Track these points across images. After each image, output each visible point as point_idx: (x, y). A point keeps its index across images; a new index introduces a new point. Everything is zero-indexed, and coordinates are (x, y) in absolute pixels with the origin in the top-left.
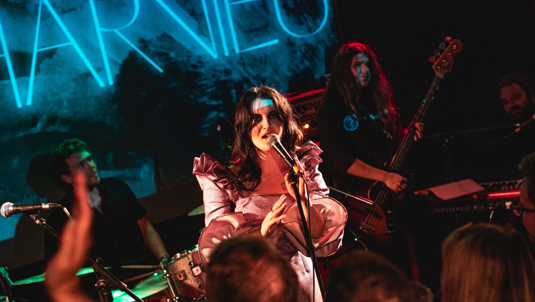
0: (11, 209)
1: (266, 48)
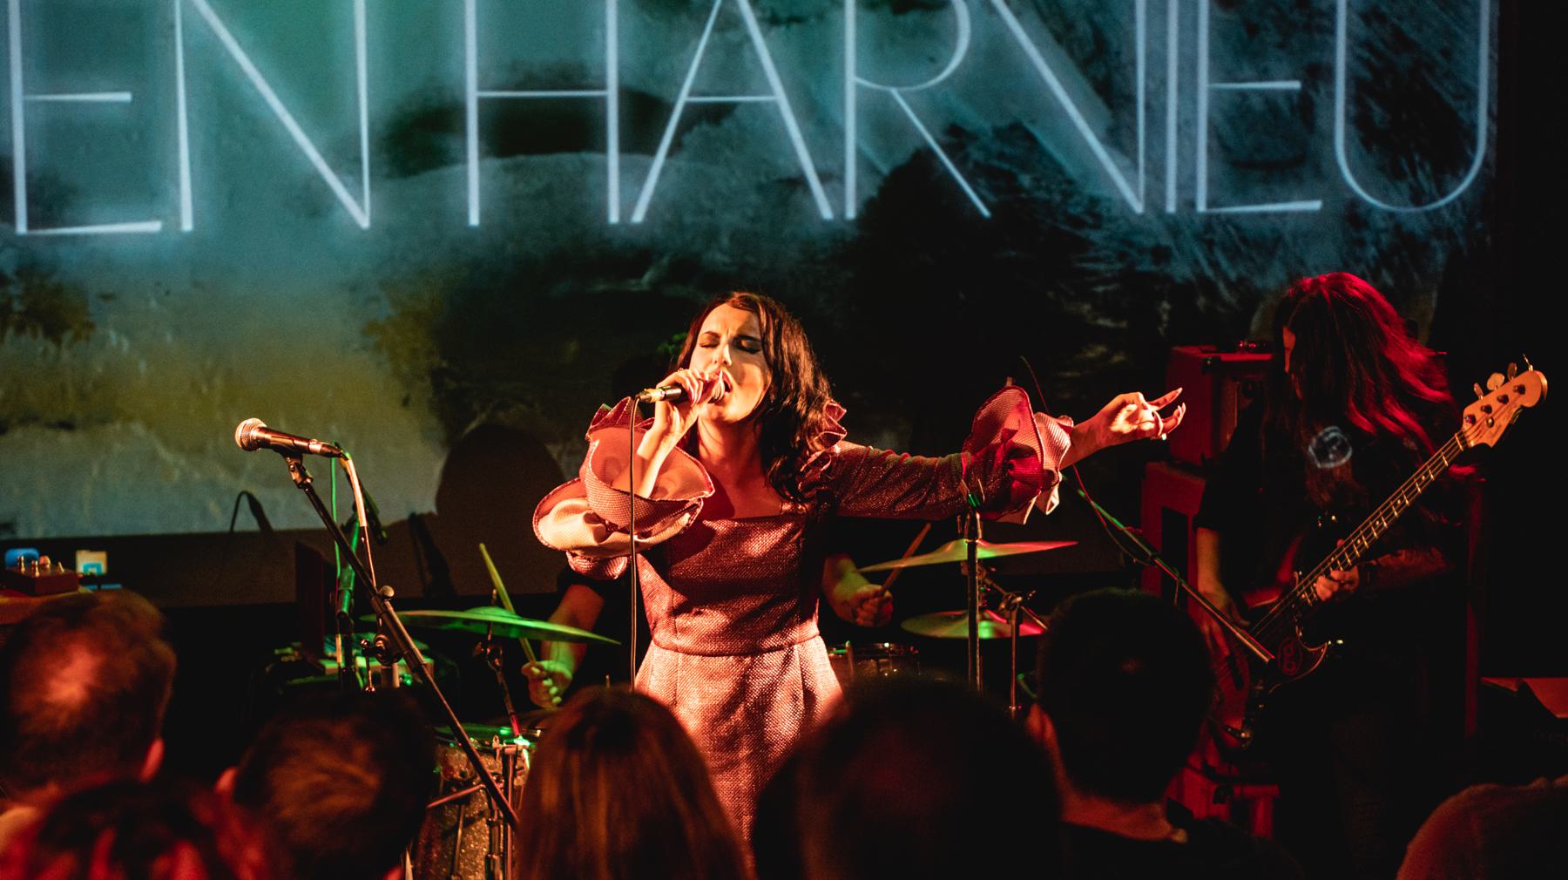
0: (255, 434)
1: (1283, 214)
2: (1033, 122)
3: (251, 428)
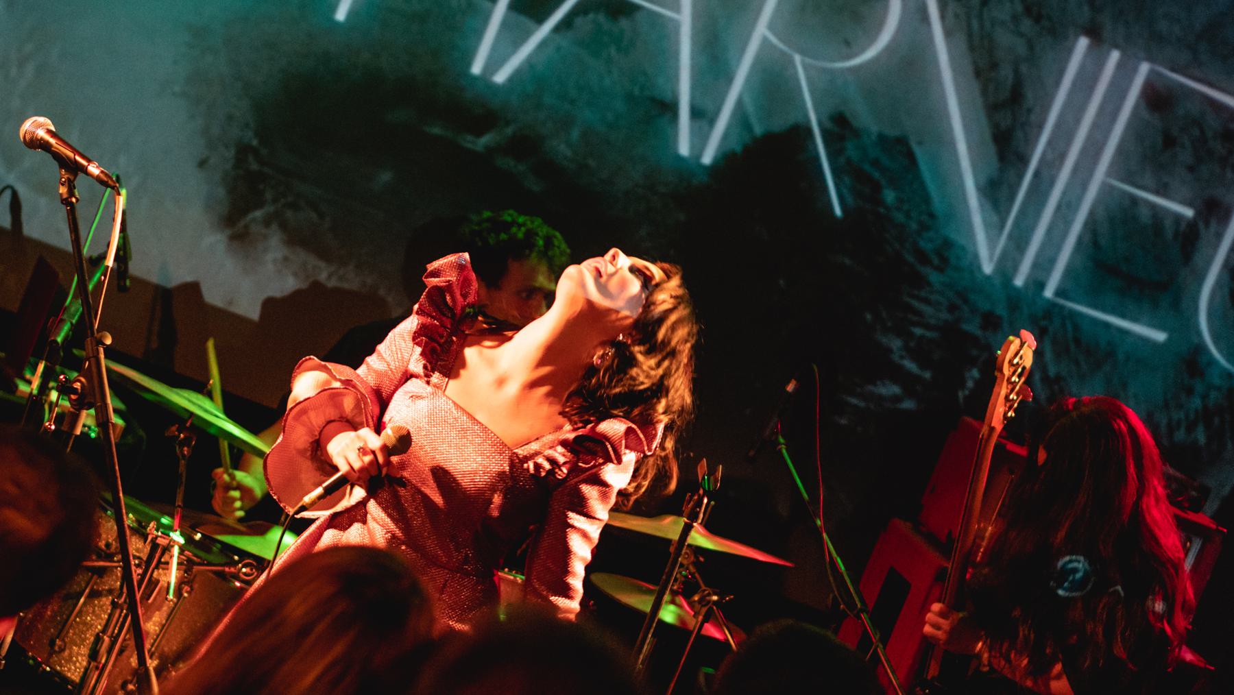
0: (41, 133)
2: (920, 143)
3: (40, 126)
